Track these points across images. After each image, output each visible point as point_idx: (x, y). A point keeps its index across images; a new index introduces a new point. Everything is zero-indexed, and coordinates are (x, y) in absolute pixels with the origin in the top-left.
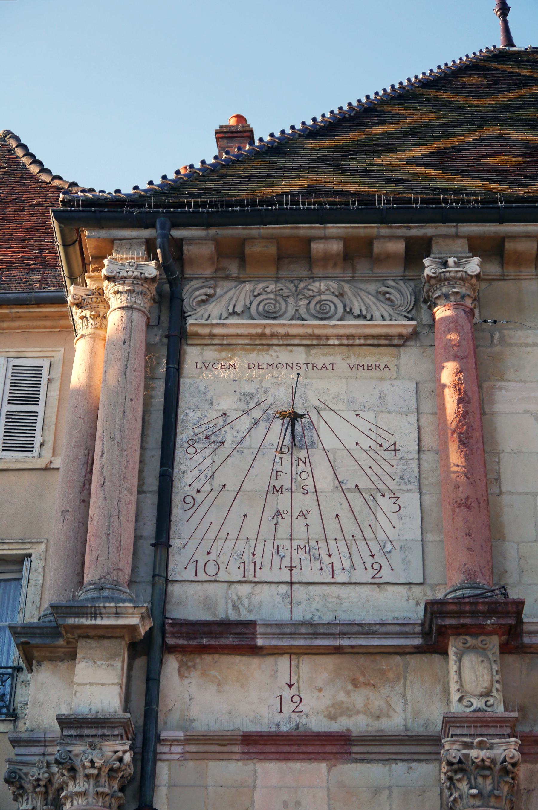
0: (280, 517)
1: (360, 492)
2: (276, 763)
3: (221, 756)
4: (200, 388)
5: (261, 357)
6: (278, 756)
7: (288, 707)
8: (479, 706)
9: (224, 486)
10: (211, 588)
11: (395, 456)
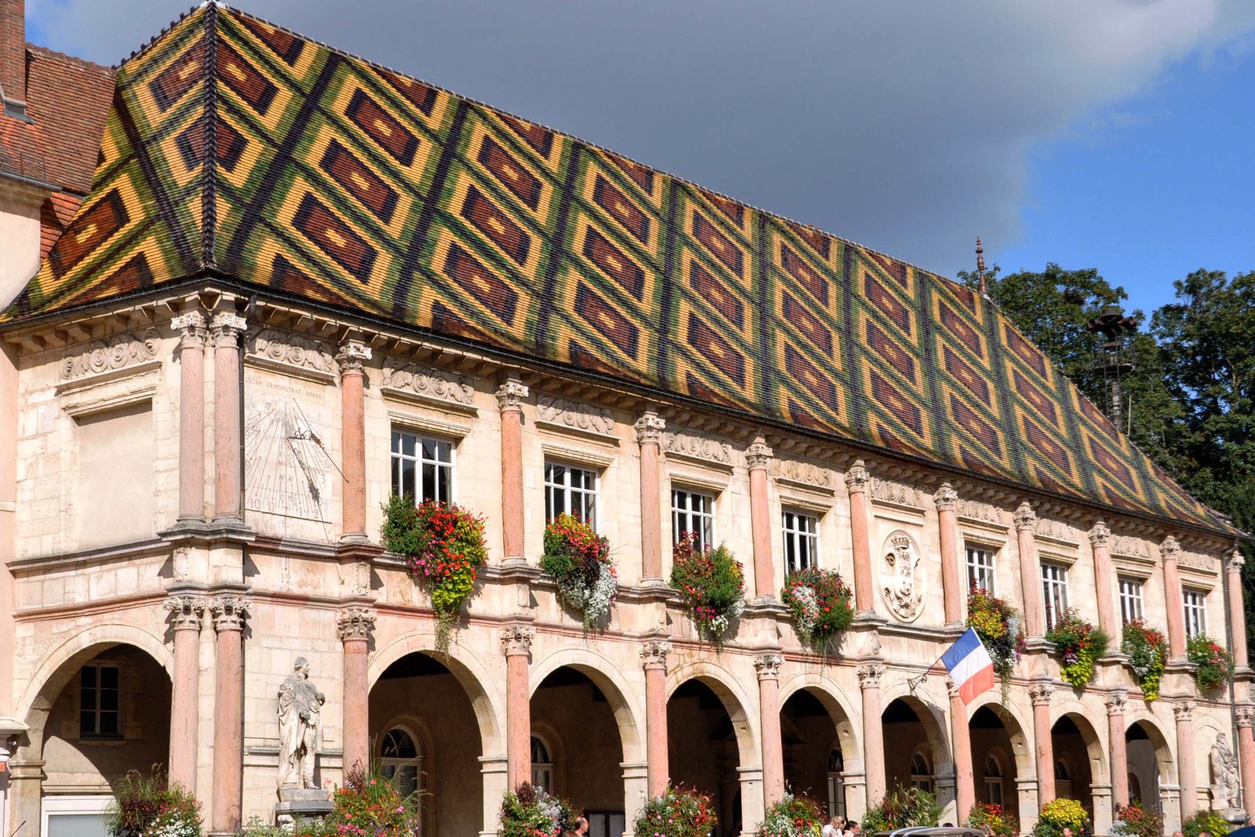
7: (285, 580)
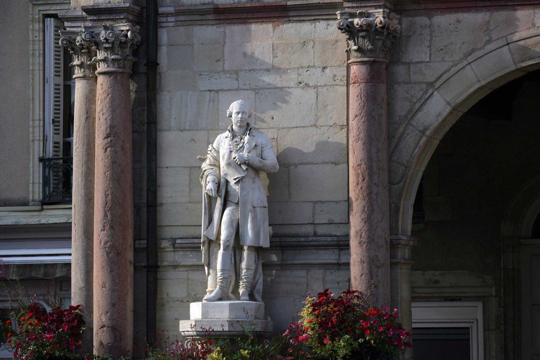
2: (238, 25)
3: (203, 23)
6: (239, 21)
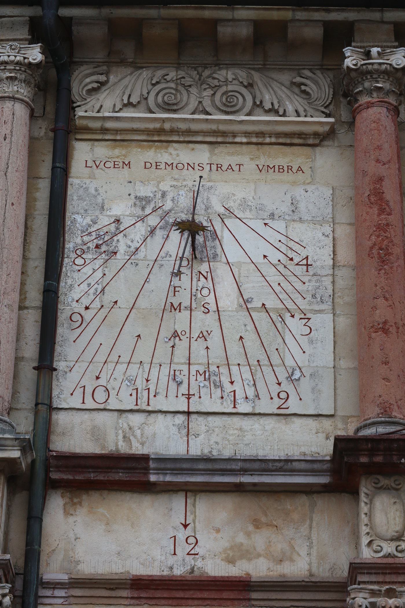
0: (177, 338)
1: (267, 311)
4: (90, 190)
5: (159, 155)
6: (170, 602)
7: (182, 549)
8: (389, 550)
9: (116, 302)
10: (101, 418)
11: (307, 271)
